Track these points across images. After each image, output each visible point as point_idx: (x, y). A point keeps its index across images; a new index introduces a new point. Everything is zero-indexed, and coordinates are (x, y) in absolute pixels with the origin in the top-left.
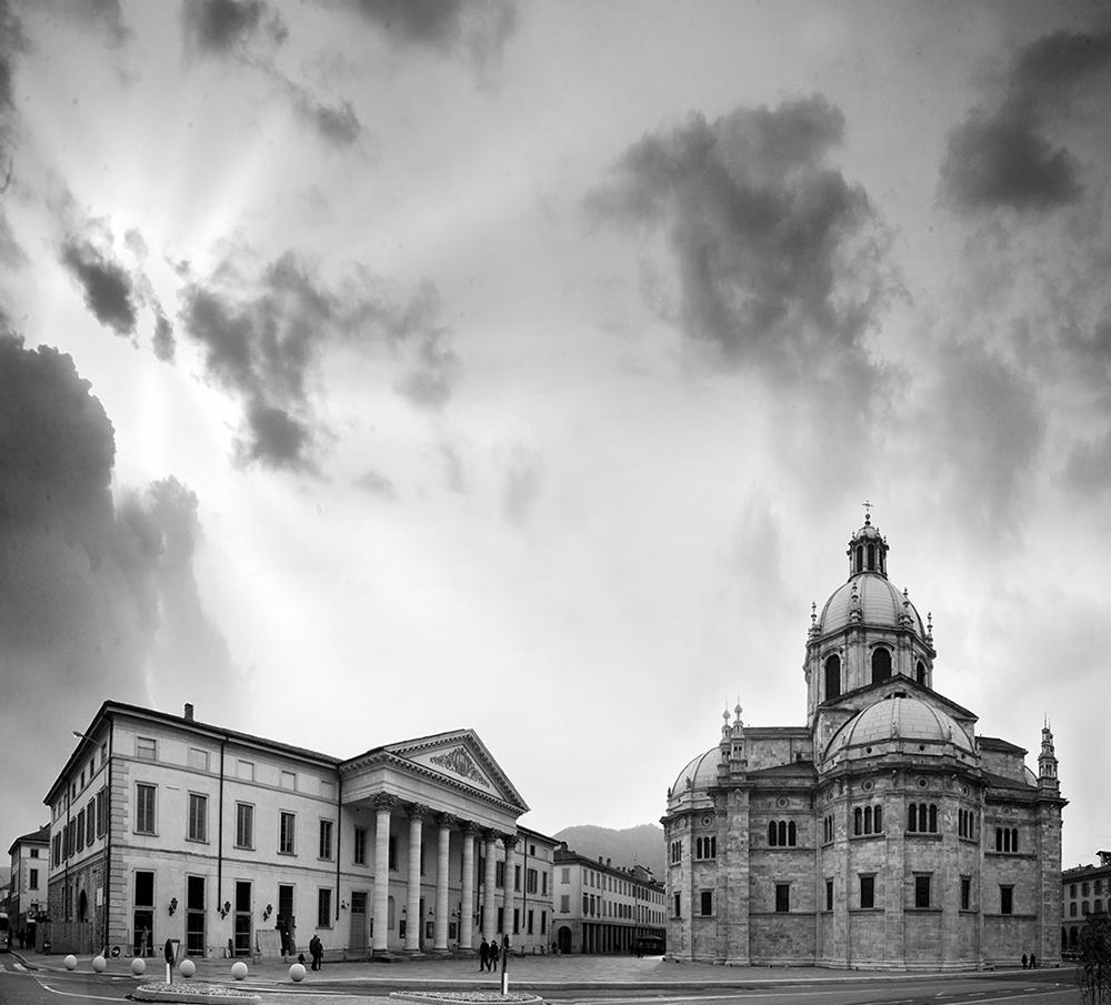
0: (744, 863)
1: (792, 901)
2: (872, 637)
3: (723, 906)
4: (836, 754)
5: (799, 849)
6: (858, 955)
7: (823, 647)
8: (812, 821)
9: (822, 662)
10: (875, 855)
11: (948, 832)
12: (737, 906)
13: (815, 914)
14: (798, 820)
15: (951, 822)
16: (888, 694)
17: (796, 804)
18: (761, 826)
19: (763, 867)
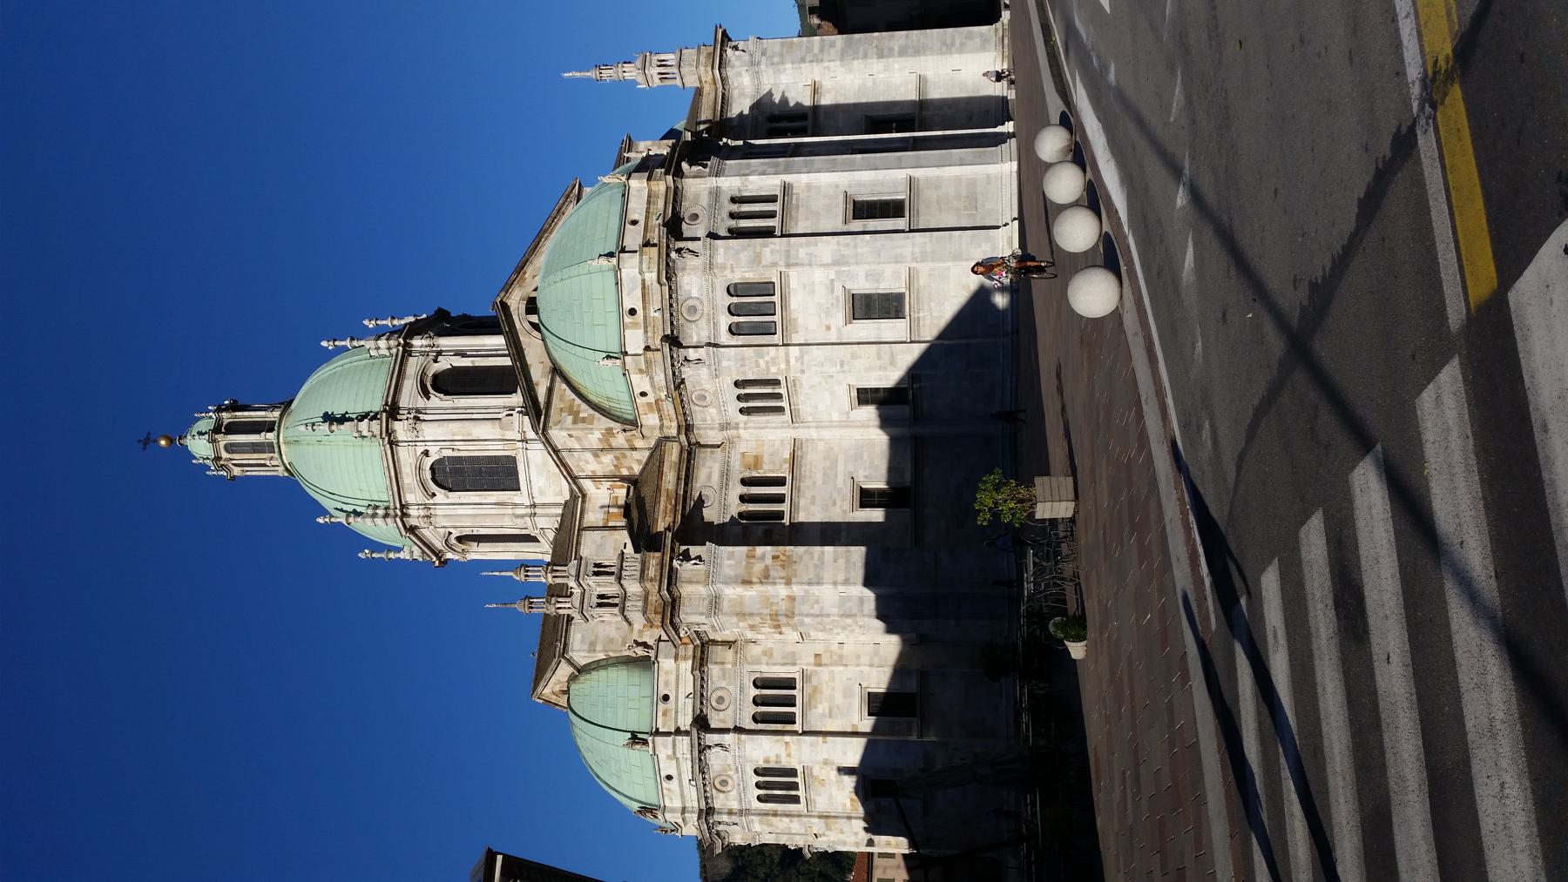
0: (816, 556)
2: (409, 396)
7: (410, 498)
9: (441, 496)
10: (812, 292)
14: (738, 472)
16: (528, 327)
17: (709, 477)
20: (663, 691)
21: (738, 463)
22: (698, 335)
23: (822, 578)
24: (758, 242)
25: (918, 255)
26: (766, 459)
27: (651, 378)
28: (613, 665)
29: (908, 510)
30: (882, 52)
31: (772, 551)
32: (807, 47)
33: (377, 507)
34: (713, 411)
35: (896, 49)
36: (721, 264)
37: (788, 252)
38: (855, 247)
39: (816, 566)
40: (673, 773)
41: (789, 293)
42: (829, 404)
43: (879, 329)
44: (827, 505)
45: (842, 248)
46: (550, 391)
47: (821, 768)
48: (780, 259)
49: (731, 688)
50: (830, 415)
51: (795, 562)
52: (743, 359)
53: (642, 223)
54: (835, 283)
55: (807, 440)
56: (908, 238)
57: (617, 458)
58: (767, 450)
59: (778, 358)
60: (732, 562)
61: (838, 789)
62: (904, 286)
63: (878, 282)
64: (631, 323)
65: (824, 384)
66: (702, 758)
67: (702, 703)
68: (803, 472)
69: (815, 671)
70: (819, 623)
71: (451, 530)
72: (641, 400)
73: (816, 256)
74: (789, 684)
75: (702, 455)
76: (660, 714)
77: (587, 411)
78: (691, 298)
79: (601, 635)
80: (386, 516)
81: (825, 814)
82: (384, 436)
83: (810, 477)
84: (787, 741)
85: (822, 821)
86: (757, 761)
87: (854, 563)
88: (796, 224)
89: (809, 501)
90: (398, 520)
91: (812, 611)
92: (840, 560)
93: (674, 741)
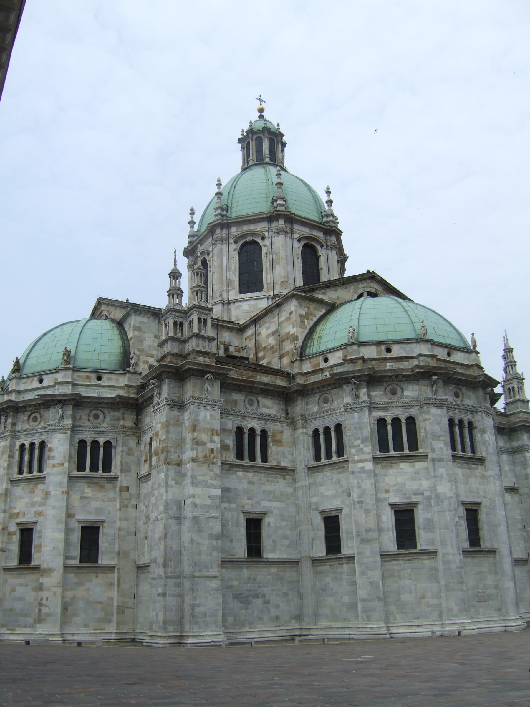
0: (213, 482)
1: (266, 542)
2: (300, 230)
3: (175, 547)
4: (334, 350)
5: (272, 468)
6: (398, 616)
7: (234, 229)
8: (287, 432)
9: (233, 246)
10: (413, 479)
12: (205, 548)
13: (297, 562)
14: (272, 428)
16: (360, 291)
17: (266, 407)
20: (105, 377)
21: (276, 427)
22: (376, 396)
23: (197, 486)
24: (448, 439)
26: (280, 449)
27: (340, 364)
28: (123, 343)
29: (246, 556)
31: (217, 448)
33: (227, 211)
34: (316, 409)
36: (430, 412)
37: (441, 460)
38: (450, 510)
39: (206, 482)
40: (46, 383)
41: (412, 462)
42: (325, 495)
43: (388, 530)
44: (248, 493)
46: (321, 302)
47: (43, 490)
49: (105, 425)
50: (315, 496)
51: (209, 466)
52: (360, 428)
53: (449, 359)
54: (421, 496)
55: (294, 480)
56: (458, 549)
57: (272, 347)
58: (286, 450)
59: (363, 454)
61: (26, 503)
62: (423, 548)
63: (424, 529)
64: (381, 349)
65: (341, 490)
66: (55, 403)
67: (95, 403)
68: (271, 475)
69: (116, 487)
70: (159, 485)
71: (211, 255)
72: (321, 359)
73: (441, 481)
74: (107, 468)
75: (281, 402)
76: (88, 374)
77: (309, 324)
78: (402, 391)
79: (146, 335)
80: (222, 216)
81: (9, 494)
82: (275, 212)
83: (268, 481)
84: (65, 465)
85: (4, 492)
86: (51, 442)
87: (208, 512)
88: (459, 467)
89: (251, 480)
90: (220, 221)
91: (170, 479)
92: (210, 500)
93: (67, 383)
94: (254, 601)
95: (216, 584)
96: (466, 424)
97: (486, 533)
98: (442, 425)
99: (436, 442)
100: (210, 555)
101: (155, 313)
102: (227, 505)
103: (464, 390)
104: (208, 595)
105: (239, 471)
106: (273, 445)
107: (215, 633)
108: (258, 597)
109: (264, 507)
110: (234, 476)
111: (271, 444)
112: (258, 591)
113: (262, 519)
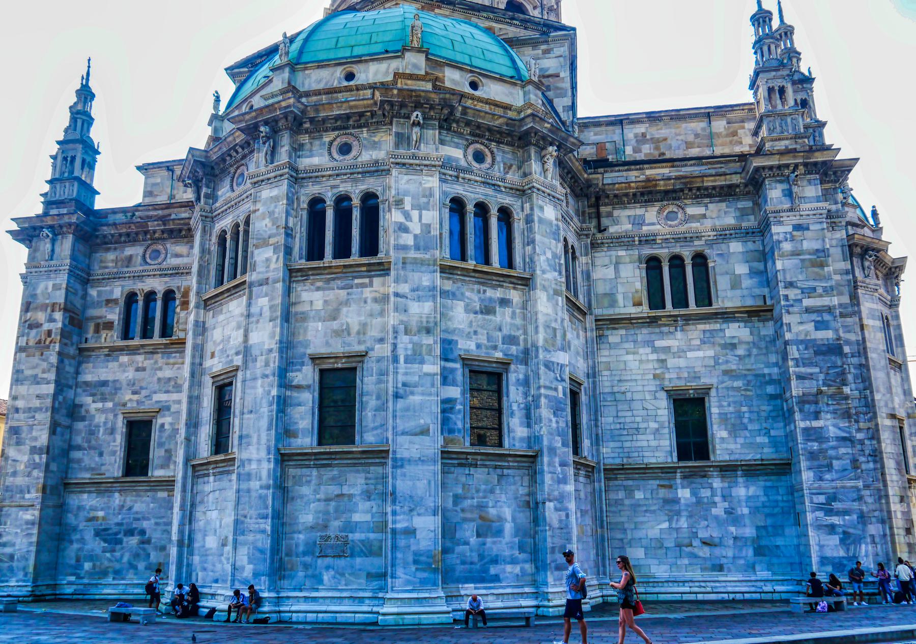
0: (45, 376)
11: (405, 248)
12: (22, 467)
15: (415, 227)
17: (177, 256)
18: (108, 301)
19: (104, 383)
23: (22, 384)
25: (247, 468)
29: (120, 474)
30: (809, 402)
32: (814, 289)
35: (815, 424)
44: (134, 384)
45: (264, 357)
48: (259, 273)
51: (42, 354)
56: (269, 453)
60: (50, 289)
73: (258, 322)
88: (318, 289)
89: (140, 365)
94: (125, 539)
95: (33, 515)
96: (356, 202)
97: (370, 414)
98: (276, 215)
99: (261, 250)
100: (29, 474)
101: (168, 167)
102: (100, 405)
103: (365, 133)
104: (19, 531)
105: (122, 355)
106: (182, 310)
107: (20, 584)
108: (133, 535)
109: (157, 402)
110: (116, 364)
111: (178, 310)
112: (134, 526)
113: (151, 421)
